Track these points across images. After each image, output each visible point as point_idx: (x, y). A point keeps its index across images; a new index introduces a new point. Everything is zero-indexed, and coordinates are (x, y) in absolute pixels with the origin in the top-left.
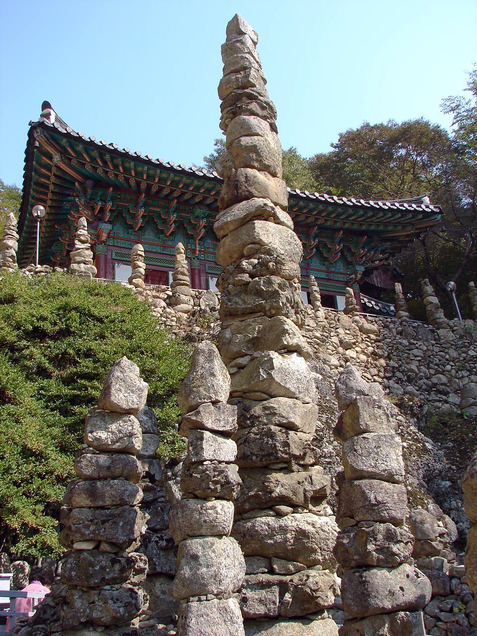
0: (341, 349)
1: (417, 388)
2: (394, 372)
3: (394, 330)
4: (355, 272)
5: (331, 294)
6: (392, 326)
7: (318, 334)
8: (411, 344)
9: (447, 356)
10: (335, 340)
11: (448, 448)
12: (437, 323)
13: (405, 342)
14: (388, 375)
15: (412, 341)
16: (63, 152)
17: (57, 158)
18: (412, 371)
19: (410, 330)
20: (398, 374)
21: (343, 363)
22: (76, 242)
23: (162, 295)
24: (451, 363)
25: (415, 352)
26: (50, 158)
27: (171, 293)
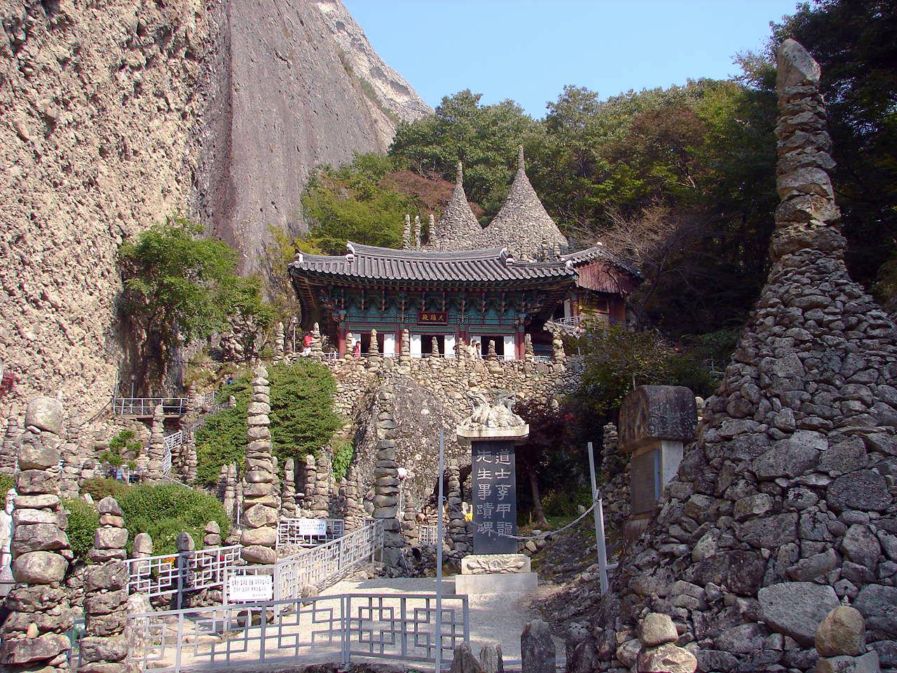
0: (467, 388)
4: (519, 319)
7: (453, 379)
10: (465, 381)
12: (555, 360)
13: (523, 376)
15: (528, 375)
23: (361, 363)
25: (528, 383)
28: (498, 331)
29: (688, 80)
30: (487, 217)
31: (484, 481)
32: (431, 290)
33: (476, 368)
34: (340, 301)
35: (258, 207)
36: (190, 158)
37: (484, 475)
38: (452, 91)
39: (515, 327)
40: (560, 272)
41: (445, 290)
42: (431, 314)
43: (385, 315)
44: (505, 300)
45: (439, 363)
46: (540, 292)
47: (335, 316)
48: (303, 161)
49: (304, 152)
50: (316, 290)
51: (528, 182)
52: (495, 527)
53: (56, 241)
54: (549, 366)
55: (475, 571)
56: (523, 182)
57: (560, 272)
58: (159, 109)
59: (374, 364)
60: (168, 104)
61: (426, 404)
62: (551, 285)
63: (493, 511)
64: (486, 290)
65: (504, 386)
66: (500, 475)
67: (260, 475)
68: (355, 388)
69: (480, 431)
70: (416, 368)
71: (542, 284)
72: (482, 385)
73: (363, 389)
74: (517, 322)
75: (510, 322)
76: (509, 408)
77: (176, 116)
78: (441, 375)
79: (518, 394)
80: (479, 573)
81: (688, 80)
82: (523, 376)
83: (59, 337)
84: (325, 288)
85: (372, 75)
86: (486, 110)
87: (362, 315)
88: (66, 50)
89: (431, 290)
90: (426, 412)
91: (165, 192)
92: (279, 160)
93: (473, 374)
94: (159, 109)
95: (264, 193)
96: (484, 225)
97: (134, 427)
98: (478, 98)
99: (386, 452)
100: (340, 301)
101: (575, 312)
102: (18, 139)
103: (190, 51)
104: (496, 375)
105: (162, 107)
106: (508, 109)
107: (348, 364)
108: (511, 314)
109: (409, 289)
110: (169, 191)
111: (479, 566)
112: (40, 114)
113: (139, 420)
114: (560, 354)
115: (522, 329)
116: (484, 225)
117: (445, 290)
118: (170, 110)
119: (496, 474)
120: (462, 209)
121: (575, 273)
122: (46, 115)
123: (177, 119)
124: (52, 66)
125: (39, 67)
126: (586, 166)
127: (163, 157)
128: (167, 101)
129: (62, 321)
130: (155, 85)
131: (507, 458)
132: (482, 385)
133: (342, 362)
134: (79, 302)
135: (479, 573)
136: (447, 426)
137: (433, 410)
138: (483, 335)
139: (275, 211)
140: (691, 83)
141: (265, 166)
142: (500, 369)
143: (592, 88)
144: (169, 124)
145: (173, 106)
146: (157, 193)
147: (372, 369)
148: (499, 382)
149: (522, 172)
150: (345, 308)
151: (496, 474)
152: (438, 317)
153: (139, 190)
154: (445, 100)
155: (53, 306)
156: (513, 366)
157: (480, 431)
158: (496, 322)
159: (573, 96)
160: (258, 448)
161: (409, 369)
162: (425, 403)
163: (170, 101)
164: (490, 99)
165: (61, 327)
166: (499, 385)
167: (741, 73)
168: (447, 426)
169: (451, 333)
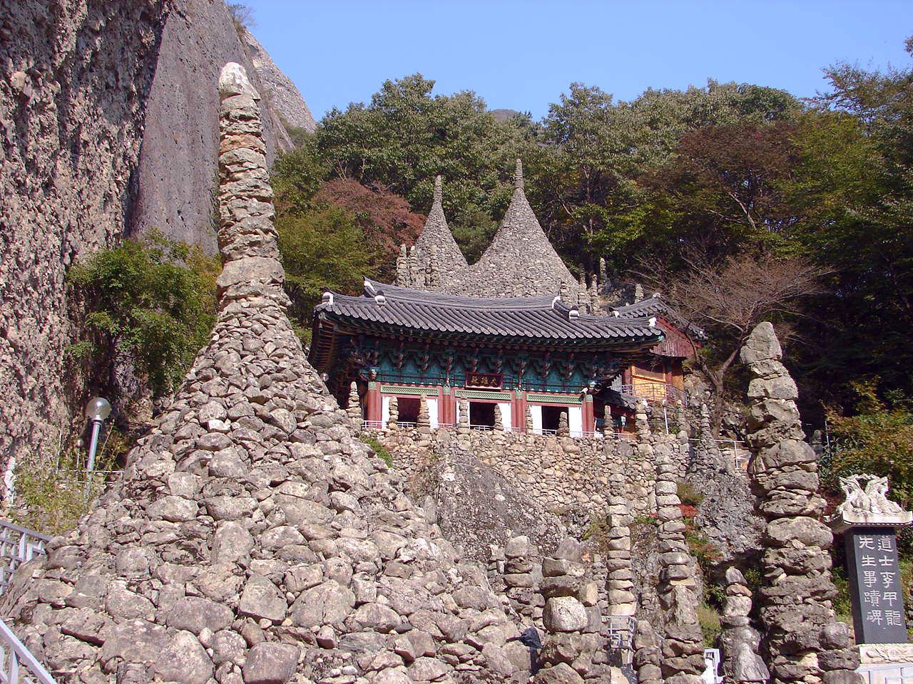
0: (540, 469)
1: (603, 496)
2: (584, 485)
3: (595, 448)
4: (588, 386)
5: (565, 405)
6: (595, 444)
7: (523, 458)
8: (608, 458)
9: (640, 468)
10: (537, 461)
11: (595, 547)
14: (578, 487)
16: (340, 324)
17: (336, 328)
18: (601, 483)
19: (610, 447)
20: (588, 486)
21: (539, 480)
22: (350, 402)
24: (642, 474)
26: (331, 330)
27: (416, 433)
29: (710, 80)
31: (869, 568)
32: (486, 346)
33: (549, 445)
34: (372, 355)
36: (131, 153)
37: (868, 561)
38: (398, 74)
40: (645, 331)
41: (504, 348)
42: (483, 375)
43: (426, 375)
44: (428, 354)
45: (504, 438)
46: (613, 354)
48: (208, 157)
50: (343, 340)
52: (883, 615)
53: (20, 259)
54: (633, 445)
55: (874, 660)
56: (521, 211)
57: (645, 331)
58: (107, 86)
59: (427, 436)
60: (118, 80)
61: (499, 488)
62: (631, 346)
63: (881, 599)
64: (552, 350)
65: (582, 469)
66: (884, 563)
67: (683, 557)
68: (405, 465)
69: (866, 516)
70: (477, 443)
71: (622, 346)
72: (557, 467)
73: (414, 467)
76: (883, 493)
77: (121, 96)
78: (508, 453)
79: (599, 479)
80: (878, 662)
81: (710, 80)
82: (603, 458)
83: (12, 386)
84: (356, 337)
86: (442, 103)
87: (396, 373)
88: (43, 8)
89: (486, 346)
90: (500, 498)
91: (108, 198)
92: (184, 155)
93: (545, 453)
94: (107, 86)
95: (169, 199)
96: (472, 257)
98: (431, 85)
99: (622, 541)
100: (372, 355)
101: (627, 380)
103: (147, 12)
104: (572, 455)
105: (111, 84)
106: (467, 104)
107: (393, 435)
109: (460, 346)
110: (110, 196)
111: (877, 654)
112: (14, 91)
114: (645, 432)
115: (590, 398)
117: (504, 348)
118: (117, 87)
119: (880, 561)
120: (438, 235)
121: (662, 334)
122: (21, 92)
123: (122, 99)
124: (28, 29)
125: (16, 29)
126: (599, 187)
127: (107, 150)
128: (116, 75)
129: (19, 366)
130: (109, 54)
132: (557, 467)
133: (385, 433)
134: (34, 342)
135: (878, 662)
136: (530, 517)
137: (508, 495)
138: (544, 404)
139: (181, 223)
140: (713, 86)
142: (577, 448)
143: (606, 89)
144: (115, 106)
145: (121, 84)
146: (99, 198)
147: (421, 443)
148: (576, 464)
149: (520, 191)
150: (378, 364)
151: (880, 561)
152: (490, 381)
153: (85, 192)
154: (388, 87)
155: (13, 345)
156: (590, 445)
157: (866, 516)
159: (580, 97)
160: (674, 529)
161: (469, 444)
162: (498, 488)
163: (120, 77)
164: (445, 88)
165: (17, 374)
166: (576, 468)
167: (831, 90)
168: (530, 517)
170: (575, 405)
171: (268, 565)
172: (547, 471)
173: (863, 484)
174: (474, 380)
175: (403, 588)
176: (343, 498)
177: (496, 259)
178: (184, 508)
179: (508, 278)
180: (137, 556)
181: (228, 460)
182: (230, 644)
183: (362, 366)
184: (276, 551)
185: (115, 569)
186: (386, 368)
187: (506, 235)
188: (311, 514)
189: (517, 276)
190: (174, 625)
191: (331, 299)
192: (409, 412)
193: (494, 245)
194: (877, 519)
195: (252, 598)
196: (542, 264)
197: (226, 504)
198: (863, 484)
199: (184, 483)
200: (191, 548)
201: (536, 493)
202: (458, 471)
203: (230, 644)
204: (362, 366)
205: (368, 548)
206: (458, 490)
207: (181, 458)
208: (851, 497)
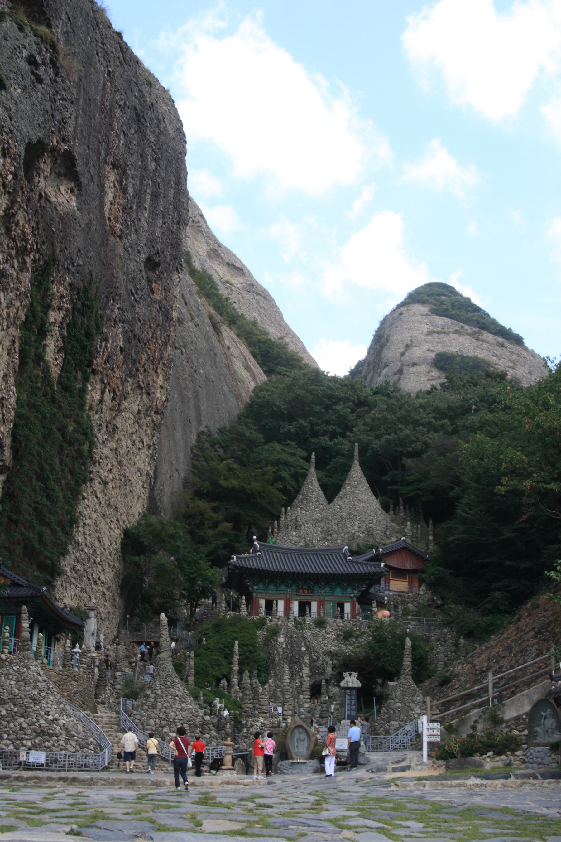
28: (341, 600)
30: (331, 491)
35: (168, 475)
39: (351, 598)
47: (251, 589)
49: (194, 424)
51: (360, 471)
56: (356, 473)
74: (352, 595)
75: (348, 595)
85: (209, 256)
90: (304, 649)
96: (330, 500)
97: (131, 647)
102: (95, 499)
108: (349, 590)
113: (133, 642)
115: (355, 599)
116: (330, 500)
131: (354, 692)
136: (315, 658)
137: (307, 648)
141: (172, 442)
149: (356, 462)
150: (257, 585)
158: (341, 595)
162: (303, 644)
168: (315, 658)
169: (315, 600)
170: (347, 602)
171: (163, 710)
172: (328, 636)
173: (350, 675)
174: (301, 591)
175: (184, 713)
176: (177, 698)
177: (340, 503)
178: (152, 700)
179: (344, 515)
180: (146, 707)
181: (159, 692)
182: (158, 721)
183: (250, 586)
184: (165, 707)
185: (143, 710)
186: (261, 586)
187: (347, 488)
188: (171, 701)
189: (349, 514)
190: (150, 718)
191: (235, 559)
192: (269, 606)
193: (341, 494)
194: (350, 685)
195: (161, 715)
196: (363, 507)
197: (159, 700)
198: (350, 675)
199: (153, 695)
200: (154, 707)
201: (322, 645)
202: (286, 637)
203: (158, 721)
204: (250, 586)
205: (180, 707)
206: (284, 646)
207: (152, 691)
208: (346, 679)
